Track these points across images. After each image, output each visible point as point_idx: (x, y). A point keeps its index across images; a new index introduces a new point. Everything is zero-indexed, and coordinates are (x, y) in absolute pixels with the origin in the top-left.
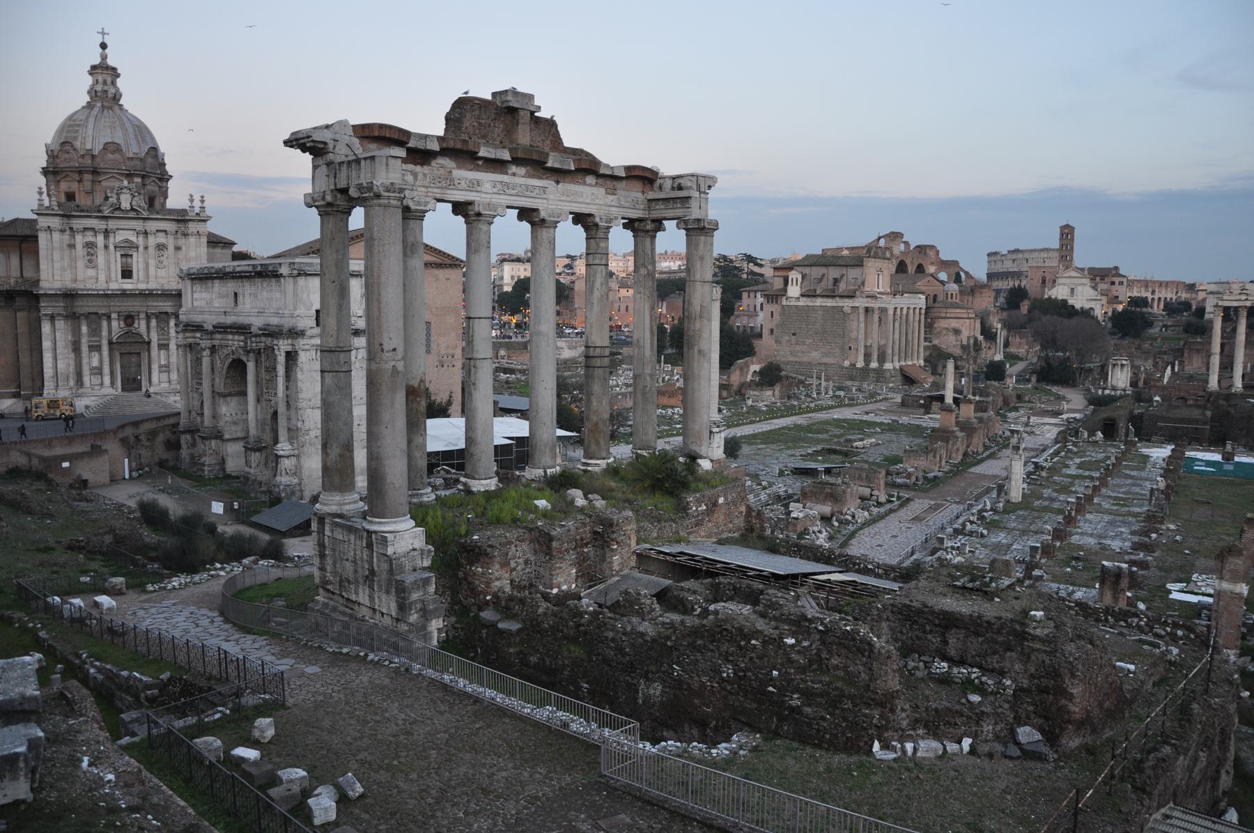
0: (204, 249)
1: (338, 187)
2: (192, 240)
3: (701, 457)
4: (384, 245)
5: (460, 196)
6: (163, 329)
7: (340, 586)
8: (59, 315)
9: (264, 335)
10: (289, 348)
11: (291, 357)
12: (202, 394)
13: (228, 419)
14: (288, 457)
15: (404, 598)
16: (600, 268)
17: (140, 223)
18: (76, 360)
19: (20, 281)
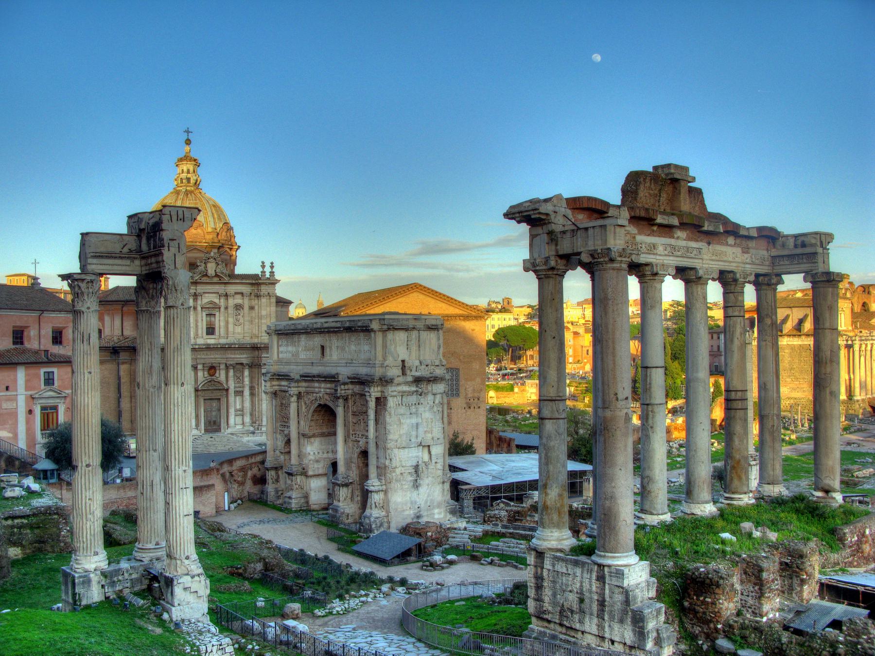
0: (273, 309)
1: (561, 253)
2: (264, 300)
4: (617, 304)
6: (239, 379)
9: (352, 383)
10: (379, 395)
11: (381, 402)
13: (311, 457)
14: (377, 492)
15: (643, 628)
16: (739, 320)
19: (121, 338)
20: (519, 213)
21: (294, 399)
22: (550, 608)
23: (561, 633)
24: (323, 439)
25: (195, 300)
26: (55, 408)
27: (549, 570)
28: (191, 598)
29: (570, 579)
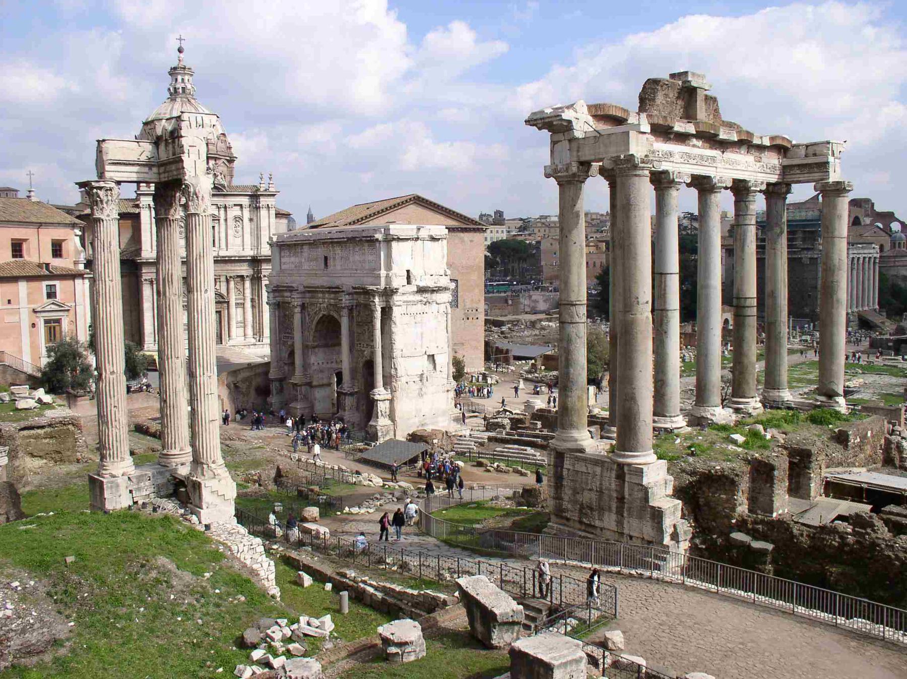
1: (583, 159)
3: (838, 395)
11: (387, 312)
13: (315, 367)
17: (222, 199)
20: (541, 119)
21: (298, 310)
22: (569, 506)
23: (580, 530)
24: (326, 349)
26: (58, 321)
27: (569, 470)
28: (218, 501)
29: (590, 478)
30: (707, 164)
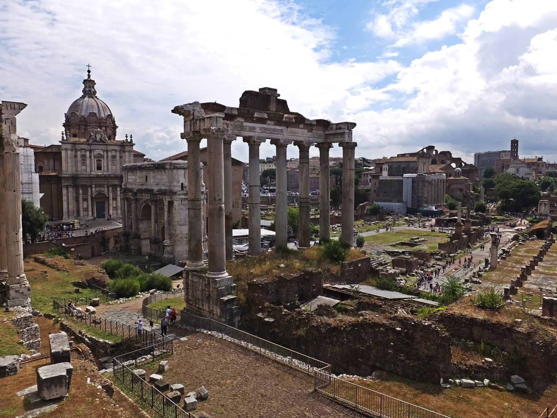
1: (195, 130)
2: (127, 154)
5: (247, 134)
6: (114, 192)
7: (195, 302)
8: (70, 186)
9: (159, 194)
10: (169, 200)
11: (171, 204)
12: (132, 219)
13: (143, 230)
14: (168, 246)
17: (105, 146)
18: (77, 205)
25: (90, 153)
30: (277, 133)
